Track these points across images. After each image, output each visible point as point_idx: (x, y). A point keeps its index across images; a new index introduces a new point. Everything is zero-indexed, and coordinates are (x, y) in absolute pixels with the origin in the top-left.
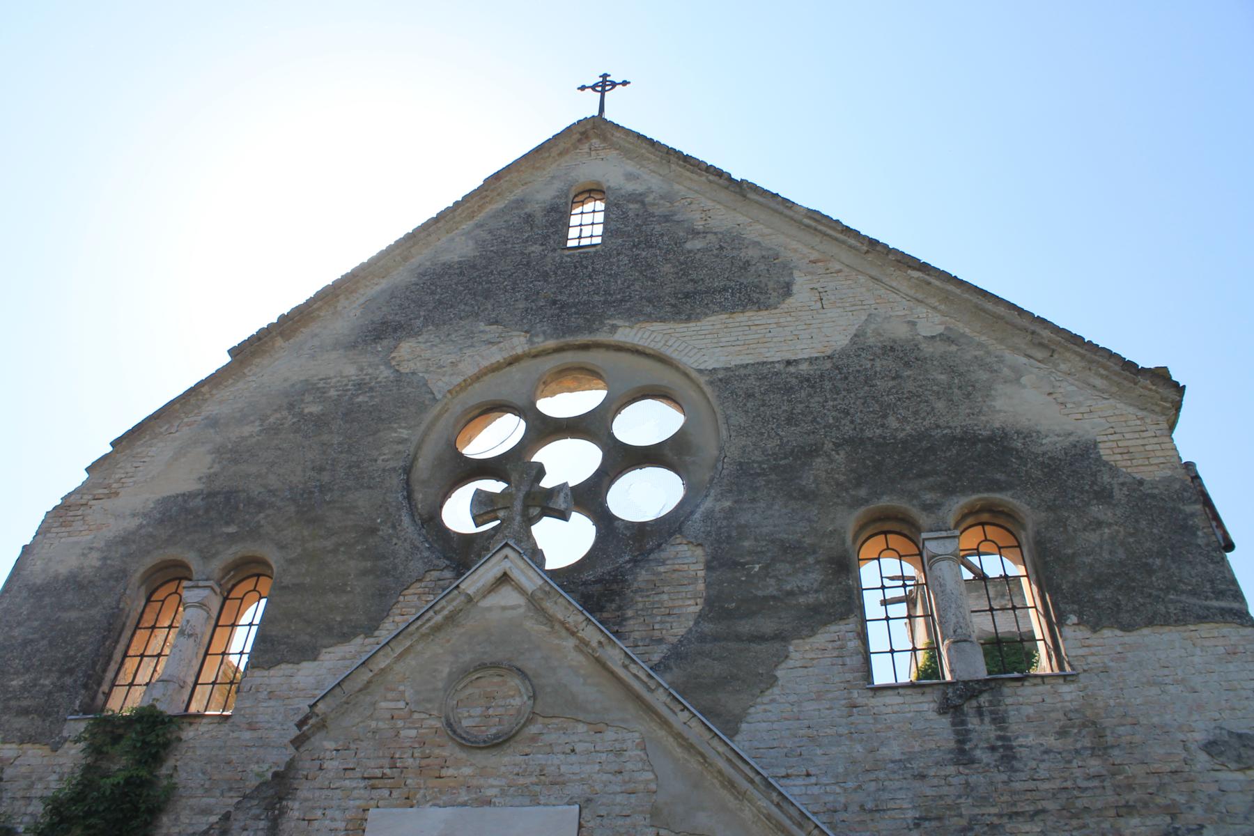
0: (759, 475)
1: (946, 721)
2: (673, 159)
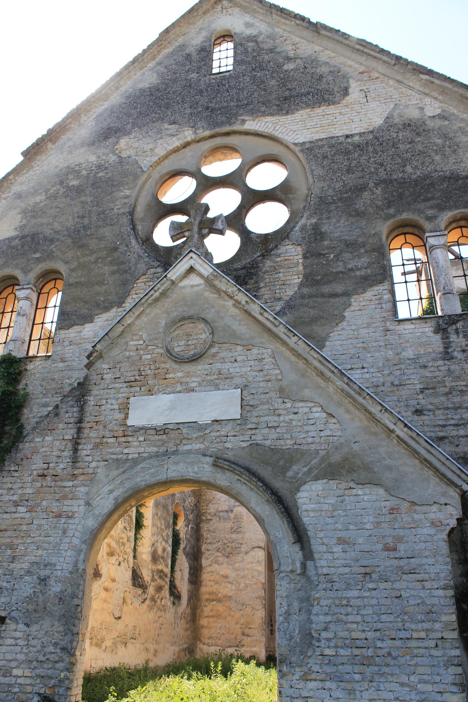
0: (331, 203)
1: (438, 337)
2: (274, 11)
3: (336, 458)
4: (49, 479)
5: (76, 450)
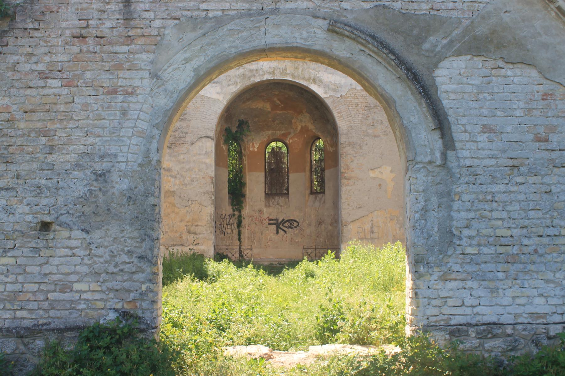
3: (482, 30)
4: (91, 42)
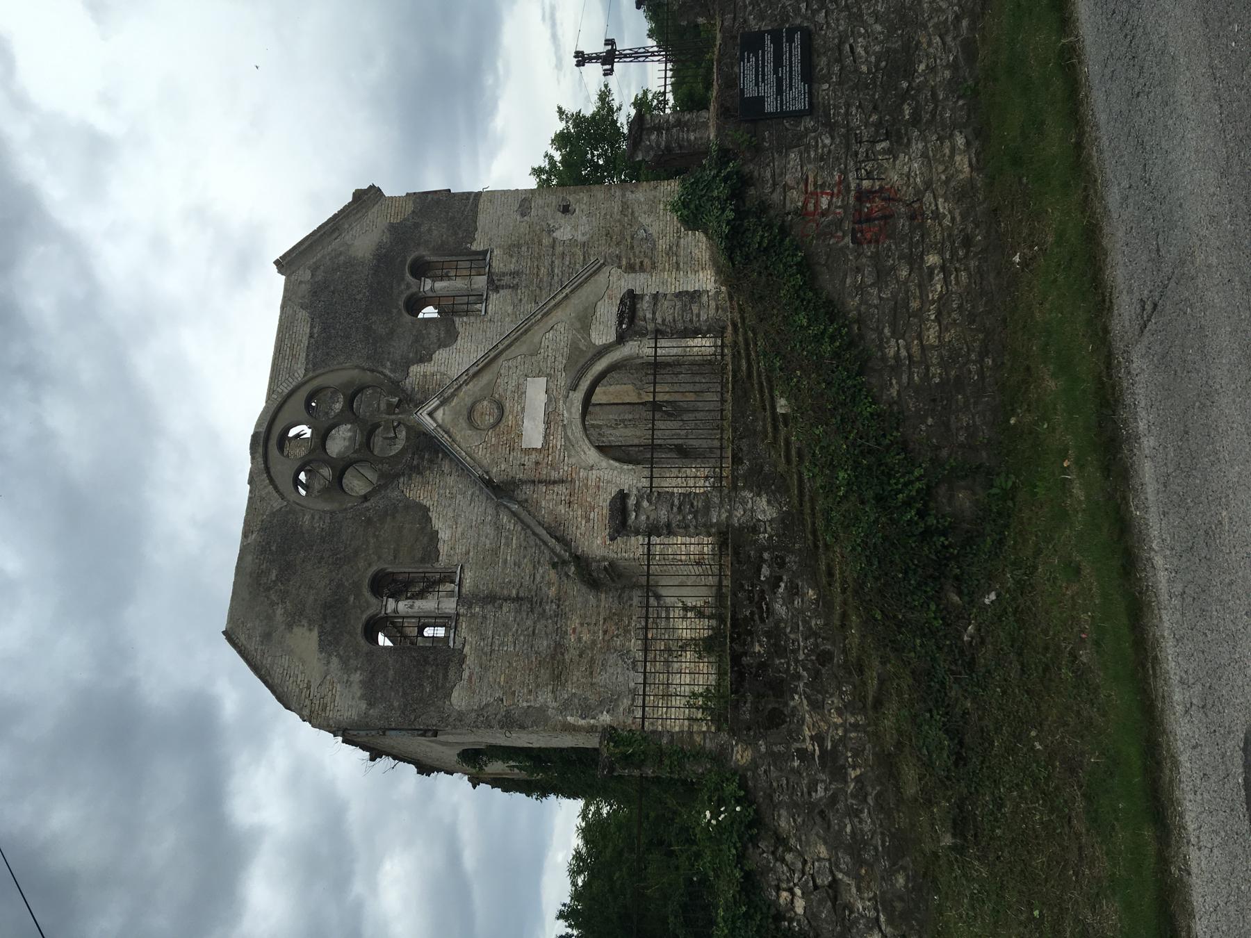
3: (578, 325)
5: (555, 482)
